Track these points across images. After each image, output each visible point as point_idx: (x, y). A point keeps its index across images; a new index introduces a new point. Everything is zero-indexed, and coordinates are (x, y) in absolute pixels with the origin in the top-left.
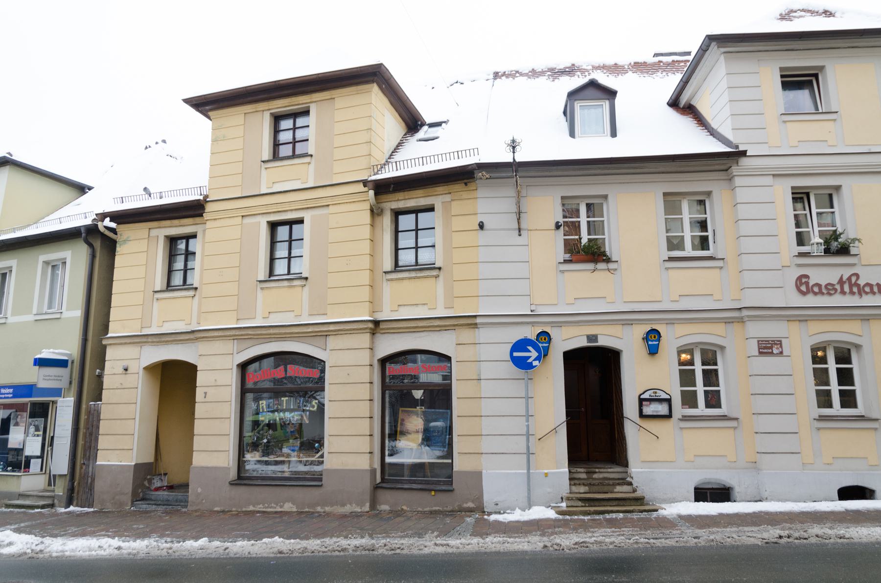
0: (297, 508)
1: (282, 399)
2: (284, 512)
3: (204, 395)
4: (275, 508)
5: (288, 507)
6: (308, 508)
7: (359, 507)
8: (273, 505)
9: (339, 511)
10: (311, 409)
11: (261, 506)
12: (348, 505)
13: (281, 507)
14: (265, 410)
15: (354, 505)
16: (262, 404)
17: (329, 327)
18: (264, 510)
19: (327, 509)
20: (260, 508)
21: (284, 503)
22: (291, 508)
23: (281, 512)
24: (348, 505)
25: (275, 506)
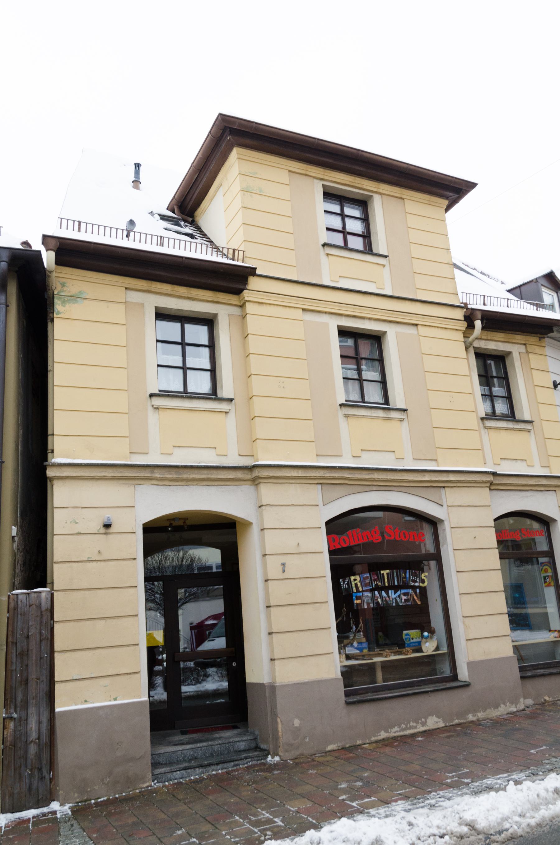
0: (444, 722)
1: (382, 572)
2: (429, 730)
3: (281, 568)
4: (416, 727)
5: (433, 722)
6: (457, 719)
7: (514, 705)
8: (412, 724)
9: (494, 715)
10: (421, 584)
11: (396, 729)
12: (502, 706)
13: (424, 724)
14: (361, 589)
15: (508, 704)
16: (355, 580)
17: (424, 476)
18: (401, 733)
19: (480, 715)
20: (395, 732)
21: (426, 718)
22: (437, 723)
23: (425, 731)
24: (502, 706)
25: (415, 724)
